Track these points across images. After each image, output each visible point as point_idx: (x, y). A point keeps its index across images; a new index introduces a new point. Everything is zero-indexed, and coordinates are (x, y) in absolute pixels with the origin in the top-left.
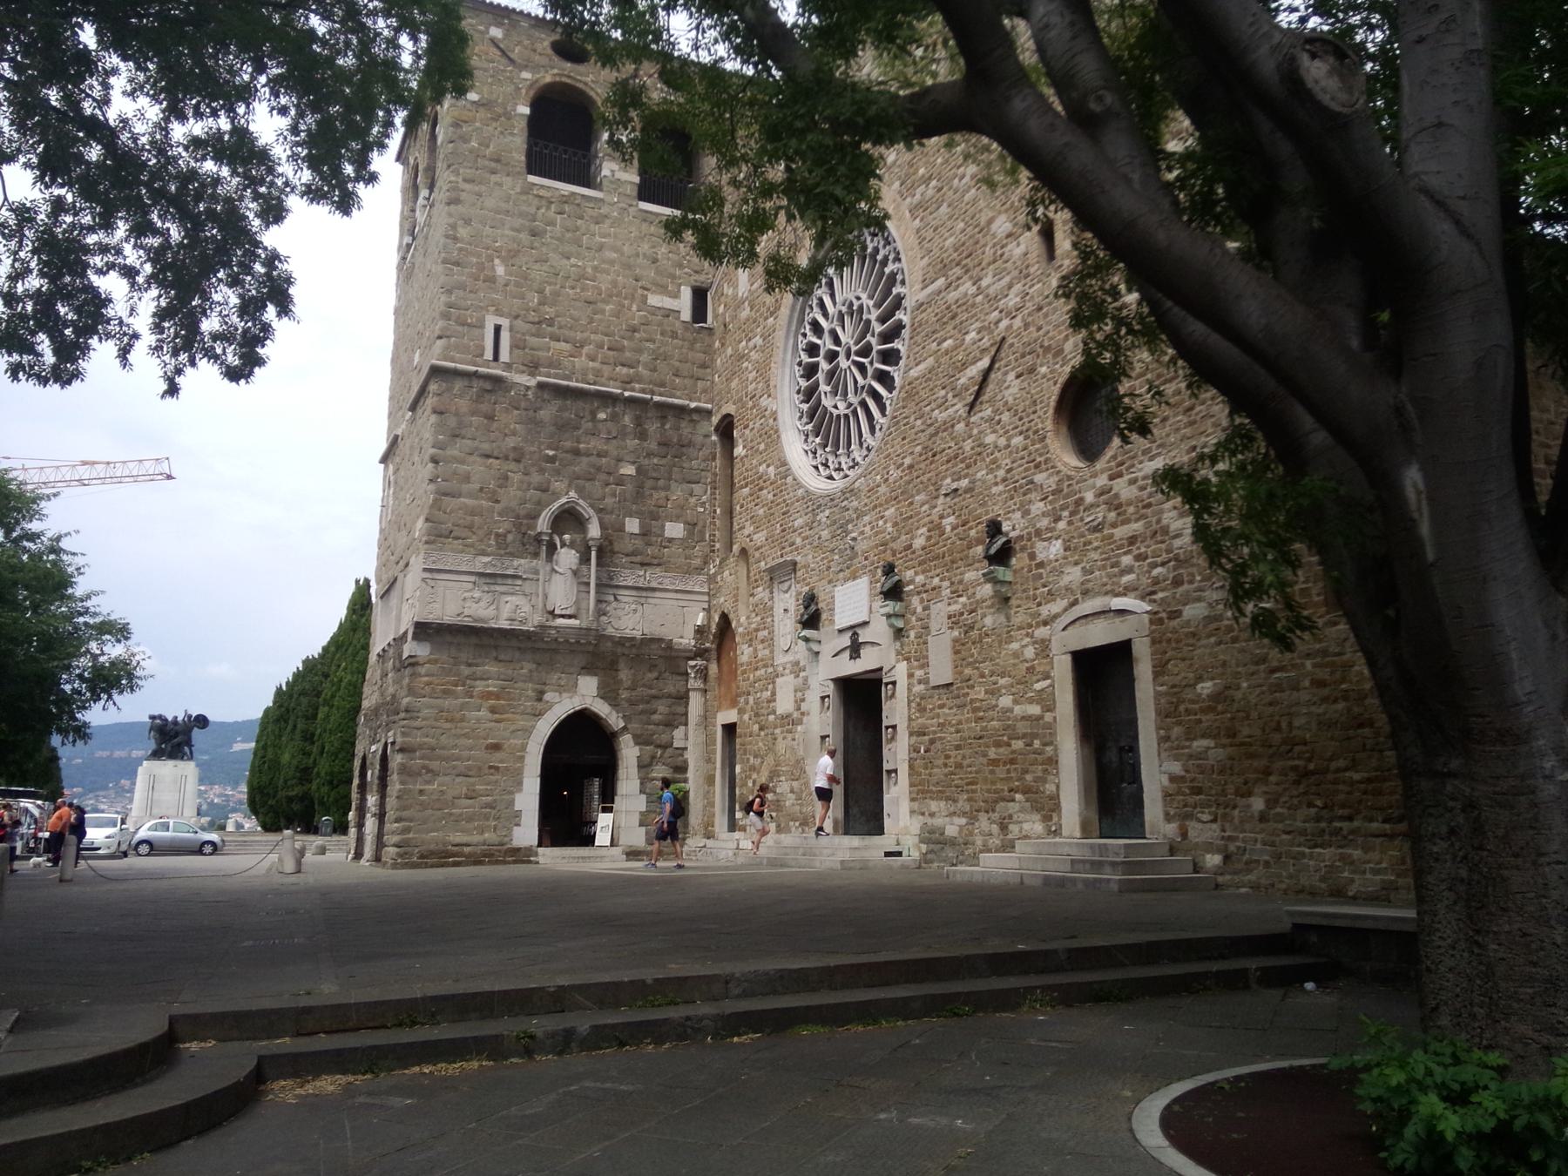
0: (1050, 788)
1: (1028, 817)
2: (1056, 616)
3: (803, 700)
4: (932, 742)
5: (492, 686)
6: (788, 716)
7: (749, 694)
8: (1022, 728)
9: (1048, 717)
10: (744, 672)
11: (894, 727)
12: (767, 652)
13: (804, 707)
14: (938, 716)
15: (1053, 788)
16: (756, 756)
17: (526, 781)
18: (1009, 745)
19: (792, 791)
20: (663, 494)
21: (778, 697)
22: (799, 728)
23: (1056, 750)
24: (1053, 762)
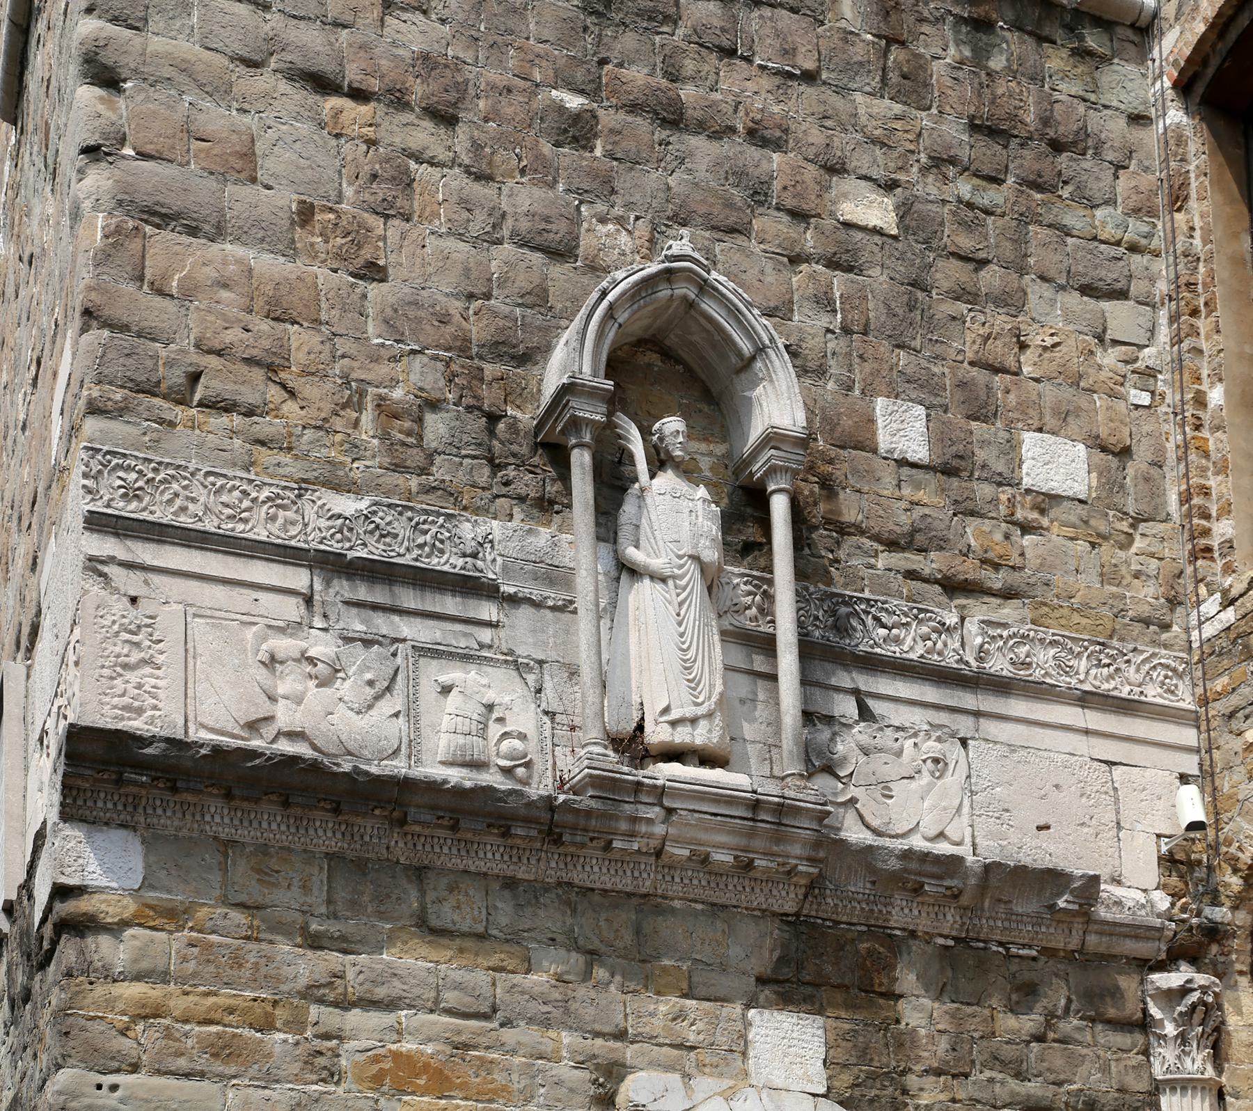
20: (1001, 321)
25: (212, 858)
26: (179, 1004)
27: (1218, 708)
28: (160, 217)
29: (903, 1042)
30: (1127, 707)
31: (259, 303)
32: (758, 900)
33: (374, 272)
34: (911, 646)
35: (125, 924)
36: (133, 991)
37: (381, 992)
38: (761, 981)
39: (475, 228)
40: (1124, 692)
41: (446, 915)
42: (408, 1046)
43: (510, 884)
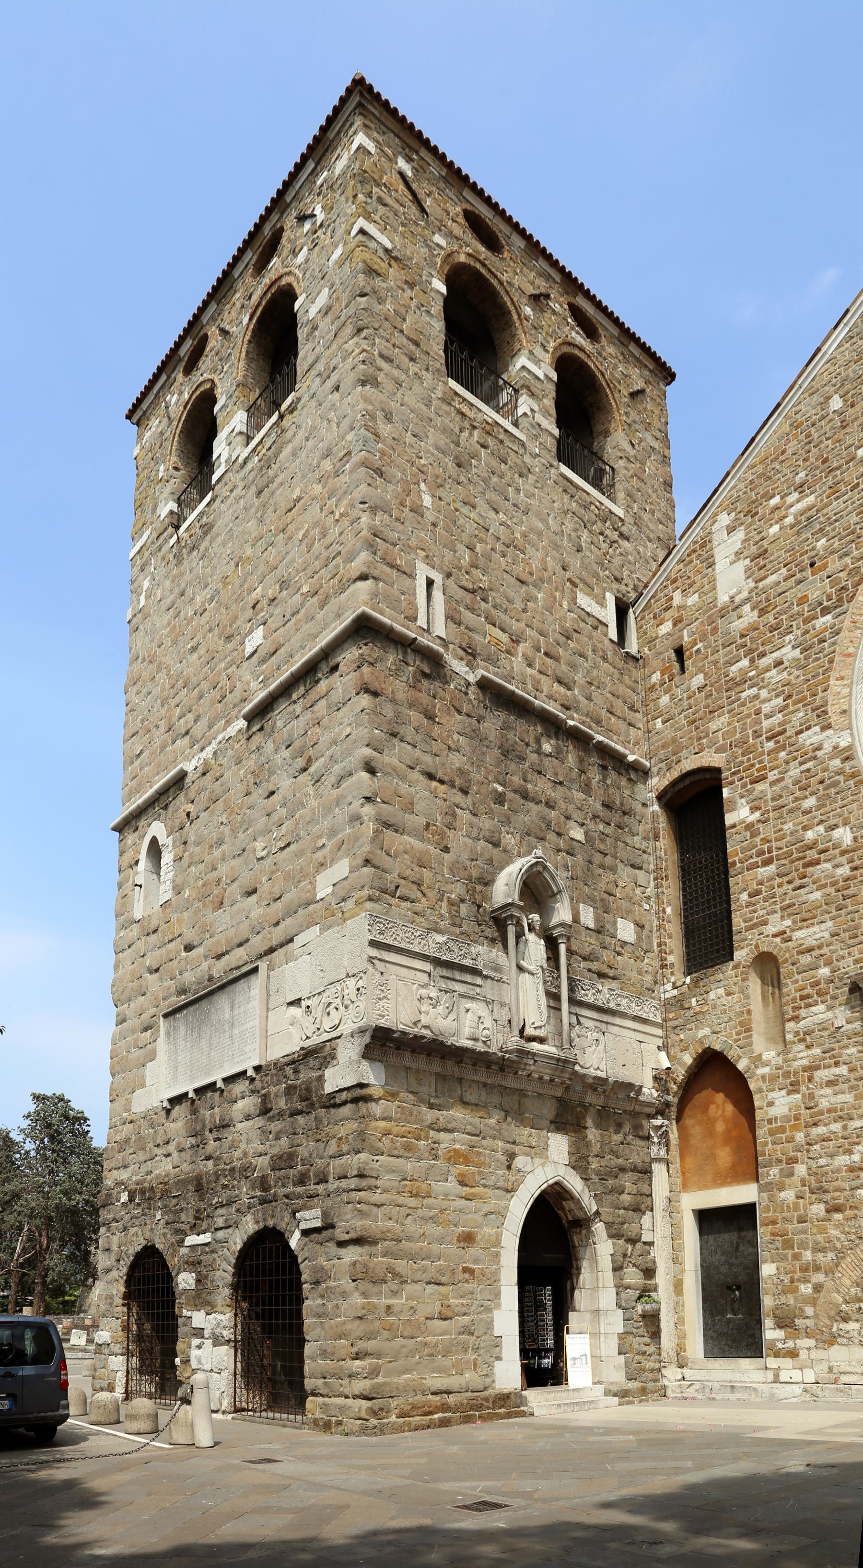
5: (459, 1142)
7: (793, 1161)
10: (782, 1130)
16: (818, 1249)
17: (503, 1289)
25: (403, 1074)
26: (396, 1130)
27: (670, 1024)
28: (387, 825)
29: (588, 1145)
30: (644, 1021)
31: (415, 860)
32: (552, 1092)
33: (446, 849)
34: (590, 999)
35: (380, 1099)
36: (382, 1124)
37: (450, 1126)
38: (551, 1122)
39: (474, 835)
40: (644, 1016)
41: (468, 1097)
42: (457, 1146)
43: (485, 1085)
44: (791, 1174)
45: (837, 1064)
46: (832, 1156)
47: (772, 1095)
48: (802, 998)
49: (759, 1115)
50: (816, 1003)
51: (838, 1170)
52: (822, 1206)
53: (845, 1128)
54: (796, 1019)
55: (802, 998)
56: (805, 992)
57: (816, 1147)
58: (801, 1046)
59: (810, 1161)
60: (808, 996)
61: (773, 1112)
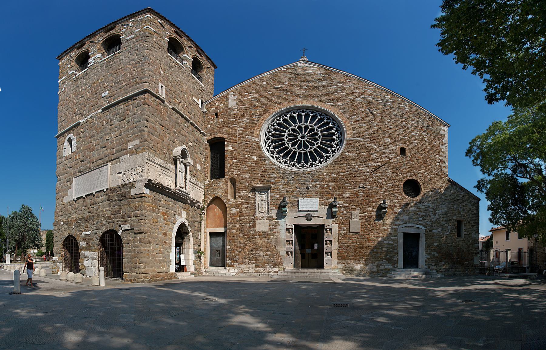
0: (395, 259)
1: (387, 264)
2: (400, 225)
3: (276, 228)
4: (349, 246)
6: (266, 232)
8: (386, 246)
9: (396, 245)
11: (331, 241)
12: (250, 212)
13: (274, 230)
14: (353, 240)
15: (396, 259)
18: (382, 249)
19: (267, 255)
21: (258, 226)
22: (272, 237)
23: (398, 251)
24: (397, 254)
44: (235, 227)
45: (248, 204)
46: (245, 224)
47: (232, 208)
48: (241, 189)
49: (228, 212)
50: (244, 190)
51: (246, 227)
52: (242, 234)
53: (249, 218)
54: (239, 193)
55: (241, 189)
56: (242, 188)
57: (242, 221)
58: (240, 199)
59: (240, 224)
60: (242, 189)
61: (232, 212)
